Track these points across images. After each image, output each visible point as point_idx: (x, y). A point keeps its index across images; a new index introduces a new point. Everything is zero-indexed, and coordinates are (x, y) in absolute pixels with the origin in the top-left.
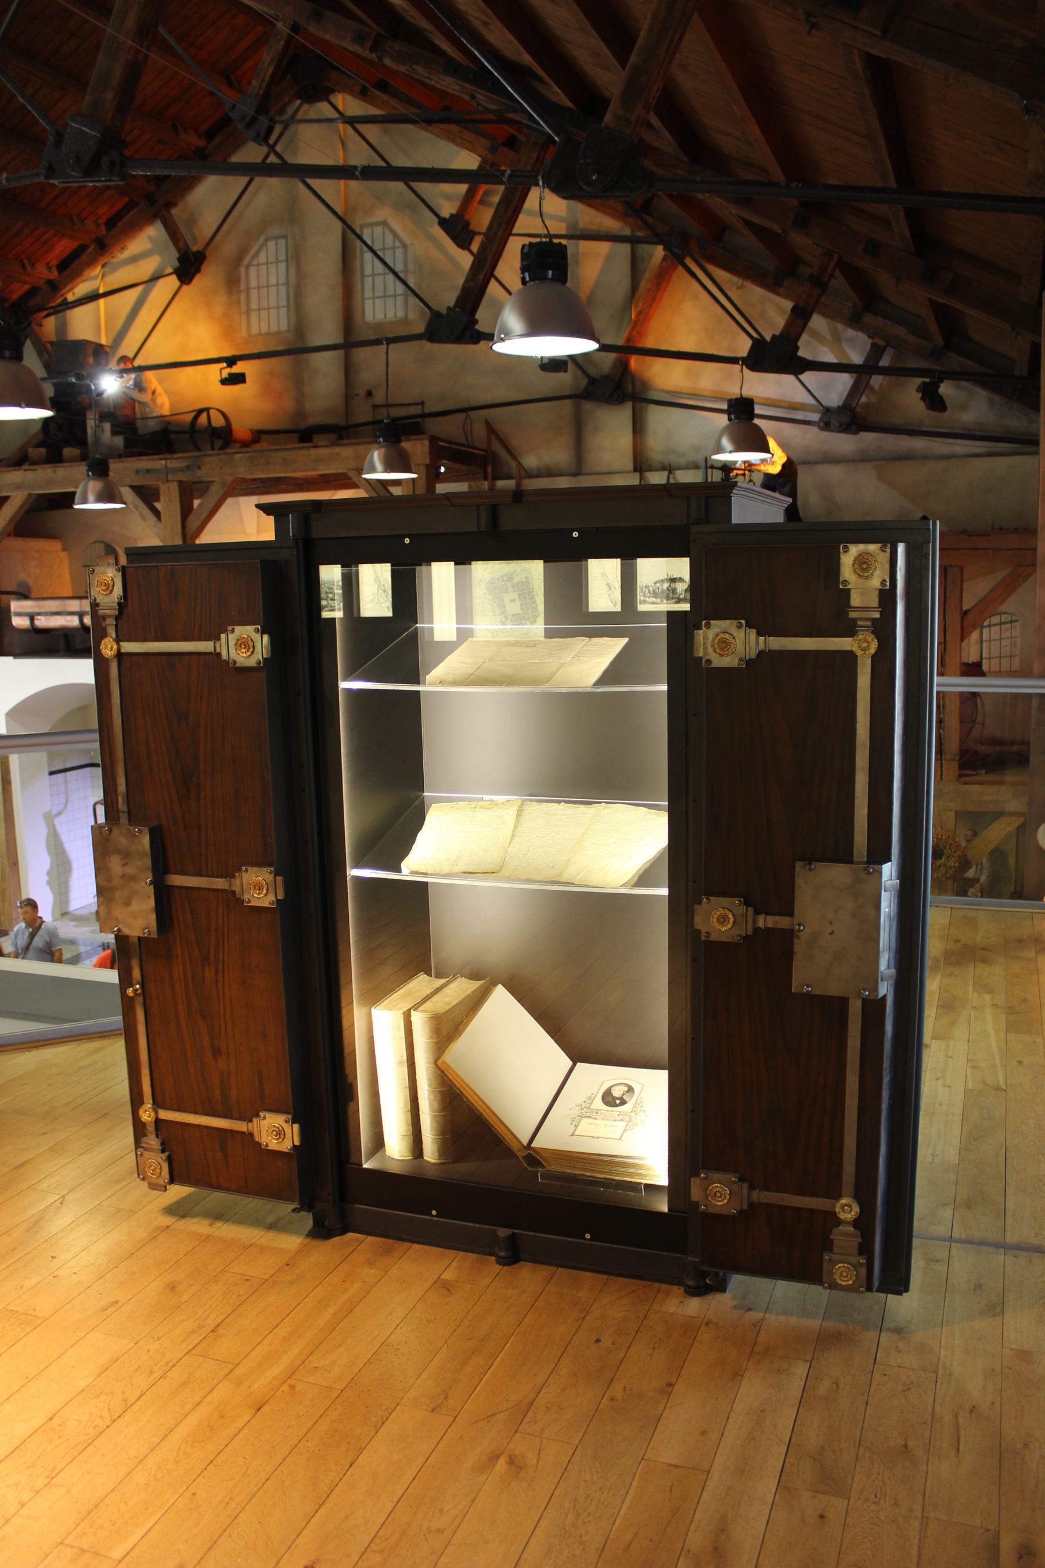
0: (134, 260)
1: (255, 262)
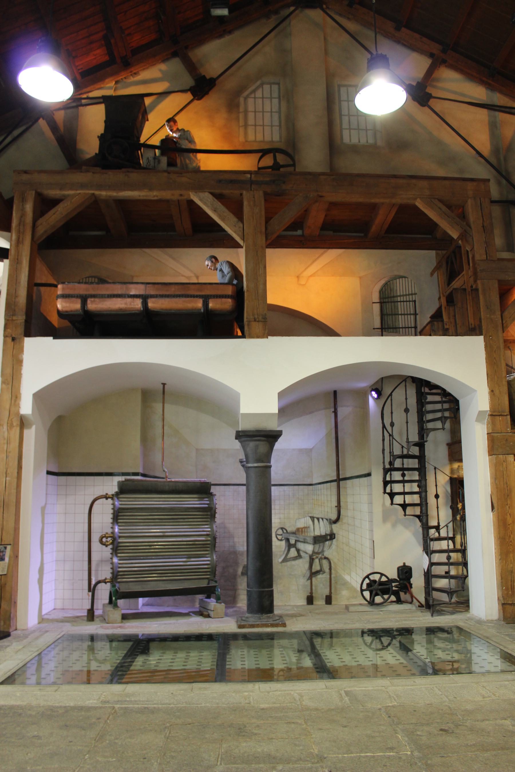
0: (145, 82)
1: (253, 96)
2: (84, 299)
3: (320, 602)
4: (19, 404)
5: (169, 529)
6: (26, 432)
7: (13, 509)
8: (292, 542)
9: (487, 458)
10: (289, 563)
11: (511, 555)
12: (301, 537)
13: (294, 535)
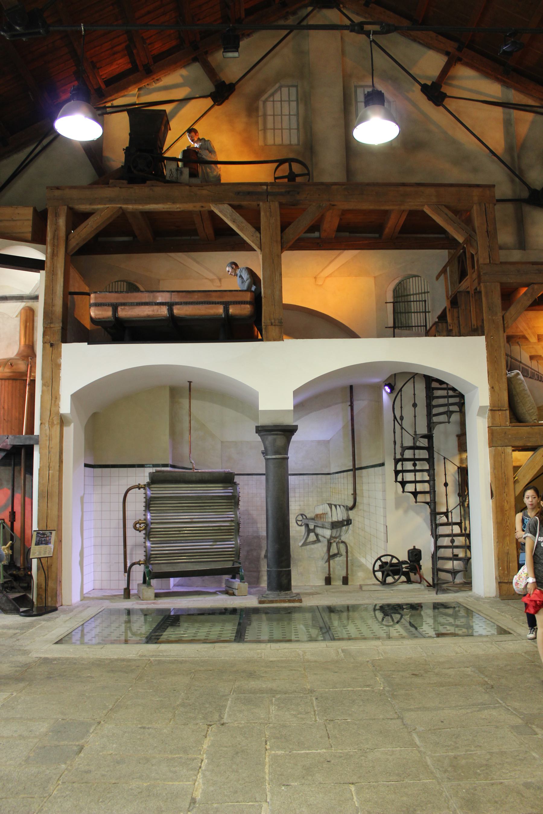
0: (166, 88)
1: (272, 99)
2: (115, 307)
3: (337, 583)
4: (59, 404)
5: (195, 516)
6: (65, 429)
7: (56, 499)
8: (311, 527)
9: (487, 449)
10: (308, 547)
11: (508, 538)
12: (319, 523)
13: (313, 521)
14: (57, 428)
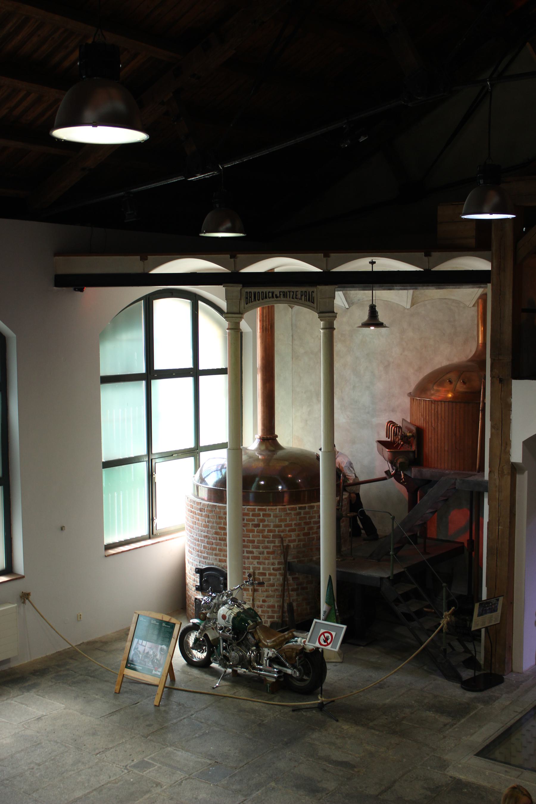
14: (508, 479)
